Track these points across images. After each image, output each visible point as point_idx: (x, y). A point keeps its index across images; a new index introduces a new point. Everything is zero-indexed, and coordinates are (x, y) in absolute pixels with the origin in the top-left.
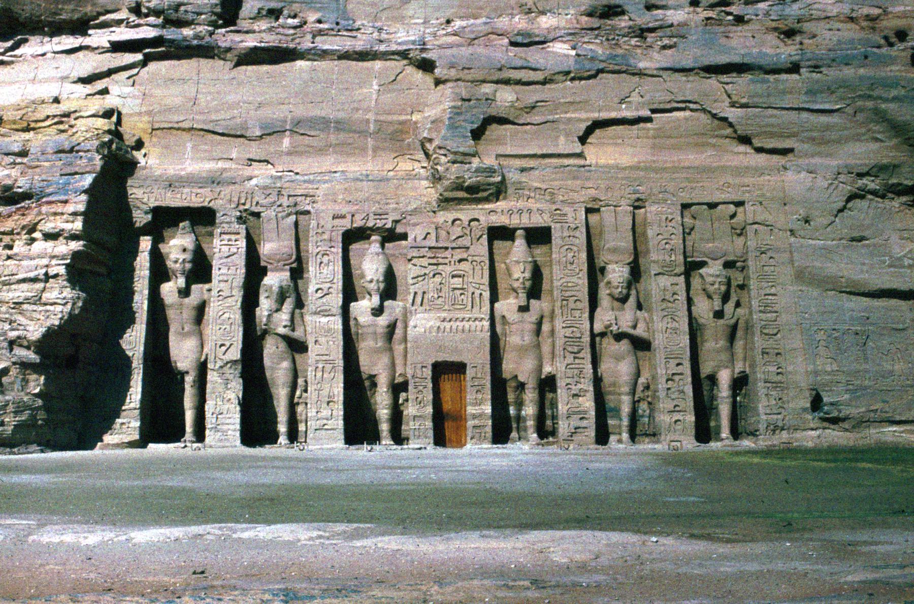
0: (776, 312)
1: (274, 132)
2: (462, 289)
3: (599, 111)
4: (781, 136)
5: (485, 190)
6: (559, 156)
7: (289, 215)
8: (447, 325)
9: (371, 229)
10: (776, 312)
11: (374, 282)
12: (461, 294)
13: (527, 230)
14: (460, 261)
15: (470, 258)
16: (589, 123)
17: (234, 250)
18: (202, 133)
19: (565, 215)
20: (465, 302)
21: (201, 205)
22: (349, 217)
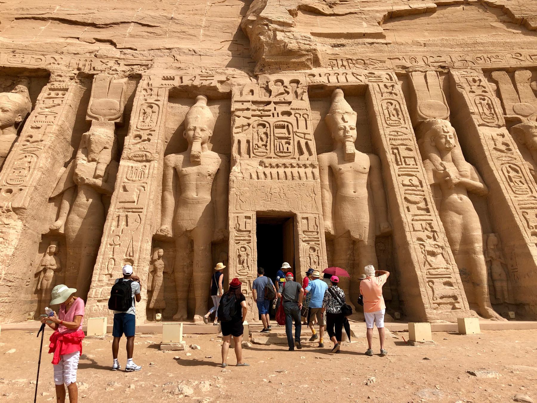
1: (122, 23)
2: (287, 138)
5: (304, 55)
6: (364, 35)
8: (274, 171)
9: (196, 87)
11: (198, 130)
12: (286, 143)
13: (343, 88)
14: (283, 113)
15: (293, 112)
16: (386, 13)
17: (57, 101)
18: (58, 22)
19: (379, 77)
20: (291, 150)
21: (36, 67)
22: (177, 79)
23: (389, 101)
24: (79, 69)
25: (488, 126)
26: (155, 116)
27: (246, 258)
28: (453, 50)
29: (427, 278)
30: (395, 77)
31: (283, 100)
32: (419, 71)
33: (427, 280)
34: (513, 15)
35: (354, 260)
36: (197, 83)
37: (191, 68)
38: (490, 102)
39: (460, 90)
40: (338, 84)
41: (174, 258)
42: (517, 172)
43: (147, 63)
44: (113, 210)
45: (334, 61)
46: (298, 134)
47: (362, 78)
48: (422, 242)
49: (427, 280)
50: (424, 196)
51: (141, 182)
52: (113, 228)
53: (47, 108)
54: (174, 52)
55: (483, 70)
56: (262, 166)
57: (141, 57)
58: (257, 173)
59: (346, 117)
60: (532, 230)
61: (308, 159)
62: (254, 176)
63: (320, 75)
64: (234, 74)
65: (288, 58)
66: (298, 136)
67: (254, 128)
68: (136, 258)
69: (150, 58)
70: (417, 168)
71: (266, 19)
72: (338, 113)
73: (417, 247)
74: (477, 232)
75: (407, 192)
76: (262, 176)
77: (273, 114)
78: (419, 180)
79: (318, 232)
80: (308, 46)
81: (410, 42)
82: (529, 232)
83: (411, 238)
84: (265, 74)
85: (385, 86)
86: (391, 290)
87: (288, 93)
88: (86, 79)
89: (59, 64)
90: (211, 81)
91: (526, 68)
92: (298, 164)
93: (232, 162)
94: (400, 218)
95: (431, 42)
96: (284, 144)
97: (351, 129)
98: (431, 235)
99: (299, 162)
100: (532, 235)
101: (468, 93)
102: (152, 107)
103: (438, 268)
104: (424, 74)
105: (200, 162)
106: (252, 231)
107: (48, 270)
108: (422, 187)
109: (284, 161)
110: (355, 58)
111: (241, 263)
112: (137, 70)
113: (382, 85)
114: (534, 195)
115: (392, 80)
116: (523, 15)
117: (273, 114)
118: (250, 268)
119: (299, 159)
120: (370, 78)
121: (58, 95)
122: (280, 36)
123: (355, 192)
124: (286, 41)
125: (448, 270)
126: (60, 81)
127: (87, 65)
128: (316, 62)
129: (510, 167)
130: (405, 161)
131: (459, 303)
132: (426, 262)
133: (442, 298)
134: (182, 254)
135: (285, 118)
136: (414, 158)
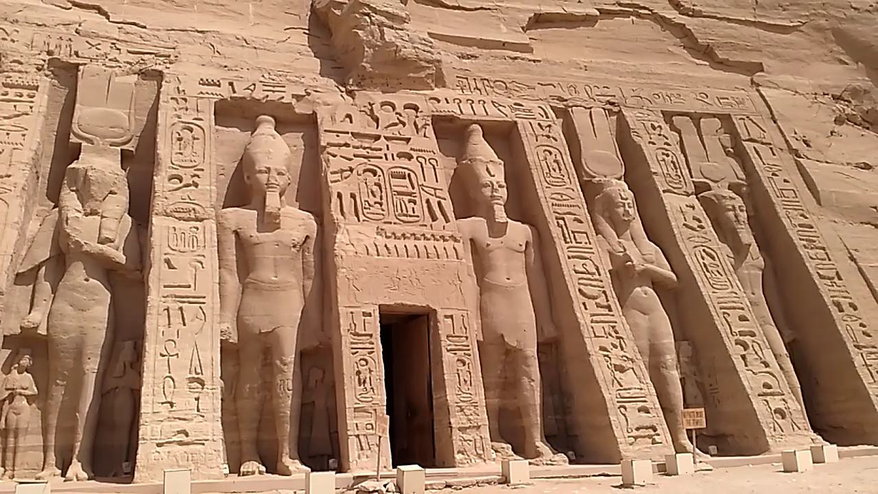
0: (824, 249)
2: (410, 194)
3: (539, 5)
4: (745, 49)
5: (424, 68)
6: (504, 45)
7: (128, 74)
8: (400, 244)
10: (824, 249)
12: (410, 201)
14: (400, 155)
15: (414, 154)
17: (22, 107)
22: (225, 84)
23: (547, 148)
24: (49, 53)
25: (675, 193)
26: (198, 145)
27: (368, 376)
28: (623, 79)
29: (618, 402)
30: (551, 113)
31: (398, 135)
32: (581, 106)
33: (619, 404)
34: (696, 39)
35: (506, 378)
36: (259, 94)
37: (245, 69)
38: (675, 160)
39: (636, 139)
40: (475, 118)
41: (237, 376)
42: (713, 258)
43: (167, 52)
44: (155, 298)
45: (463, 81)
46: (426, 189)
47: (507, 111)
48: (605, 353)
49: (619, 404)
50: (603, 287)
51: (195, 254)
52: (161, 329)
53: (5, 118)
54: (210, 39)
55: (662, 112)
56: (381, 235)
57: (155, 42)
58: (376, 246)
59: (490, 166)
60: (736, 337)
61: (444, 228)
62: (372, 250)
63: (448, 102)
64: (316, 87)
65: (400, 71)
66: (426, 192)
67: (360, 175)
68: (206, 377)
69: (170, 44)
70: (591, 248)
71: (368, 6)
72: (481, 161)
73: (601, 359)
74: (669, 341)
75: (581, 281)
76: (383, 251)
77: (386, 155)
78: (595, 265)
79: (467, 338)
80: (429, 54)
81: (566, 61)
82: (733, 339)
83: (592, 346)
84: (365, 90)
85: (539, 124)
86: (556, 419)
87: (404, 124)
88: (66, 73)
89: (13, 41)
90: (283, 94)
91: (714, 116)
92: (433, 235)
93: (327, 228)
94: (576, 318)
95: (593, 65)
96: (407, 202)
97: (500, 186)
98: (617, 342)
99: (434, 232)
100: (736, 344)
101: (648, 145)
102: (191, 130)
103: (630, 389)
104: (589, 110)
105: (279, 223)
106: (374, 336)
107: (18, 397)
108: (599, 275)
109: (409, 229)
110: (493, 80)
111: (362, 382)
112: (152, 64)
113: (535, 126)
114: (733, 290)
115: (547, 117)
116: (708, 41)
117: (386, 155)
118: (375, 391)
119: (431, 226)
120: (518, 112)
121: (21, 96)
122: (389, 35)
123: (508, 279)
124: (398, 44)
125: (643, 391)
126: (20, 72)
127: (63, 47)
128: (440, 81)
129: (704, 250)
130: (574, 236)
131: (658, 435)
132: (615, 381)
133: (637, 429)
134: (252, 370)
135: (404, 162)
136: (586, 233)
